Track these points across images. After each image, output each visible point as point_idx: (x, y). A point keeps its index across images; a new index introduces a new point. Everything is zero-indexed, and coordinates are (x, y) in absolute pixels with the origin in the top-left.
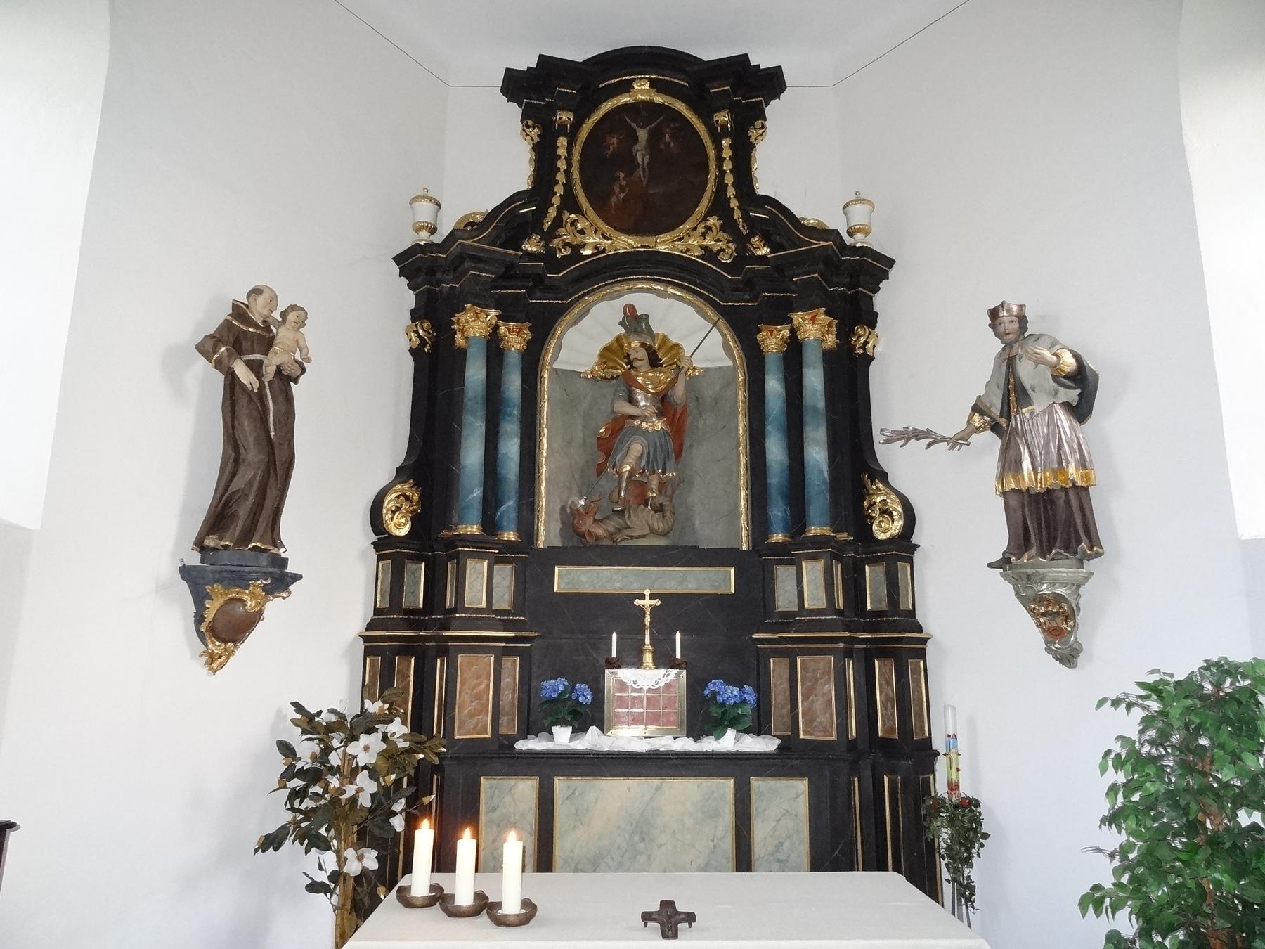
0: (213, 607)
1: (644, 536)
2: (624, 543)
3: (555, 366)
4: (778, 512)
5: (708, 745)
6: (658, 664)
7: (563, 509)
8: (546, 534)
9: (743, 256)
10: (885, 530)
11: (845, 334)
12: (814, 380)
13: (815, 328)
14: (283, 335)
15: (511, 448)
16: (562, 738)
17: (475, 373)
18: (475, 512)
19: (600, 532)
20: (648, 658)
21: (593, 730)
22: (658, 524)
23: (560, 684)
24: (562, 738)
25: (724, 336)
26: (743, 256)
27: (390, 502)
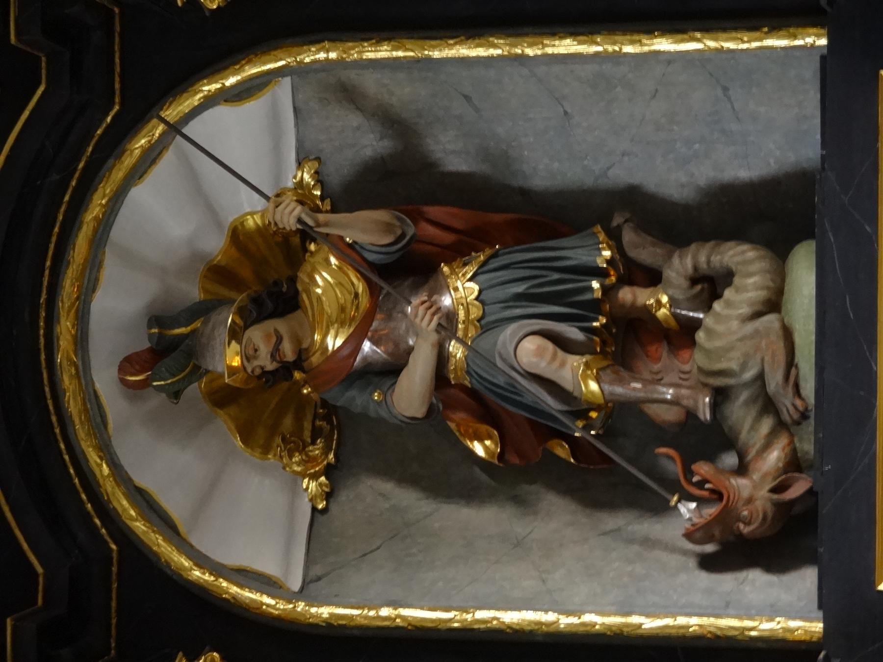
1: (787, 334)
2: (809, 388)
3: (295, 583)
7: (708, 563)
19: (775, 457)
25: (210, 102)
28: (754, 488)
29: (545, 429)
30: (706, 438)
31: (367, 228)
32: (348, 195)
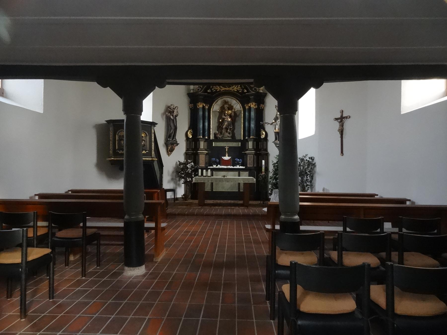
0: (169, 148)
4: (247, 134)
5: (235, 167)
6: (228, 156)
8: (212, 137)
9: (243, 91)
10: (263, 136)
11: (259, 105)
12: (253, 114)
13: (253, 105)
14: (175, 111)
15: (207, 124)
16: (215, 166)
17: (201, 113)
18: (201, 135)
20: (227, 156)
21: (219, 165)
22: (229, 135)
23: (214, 159)
24: (215, 166)
26: (243, 91)
27: (189, 133)
28: (219, 136)
29: (222, 124)
30: (221, 133)
31: (233, 114)
32: (235, 112)
